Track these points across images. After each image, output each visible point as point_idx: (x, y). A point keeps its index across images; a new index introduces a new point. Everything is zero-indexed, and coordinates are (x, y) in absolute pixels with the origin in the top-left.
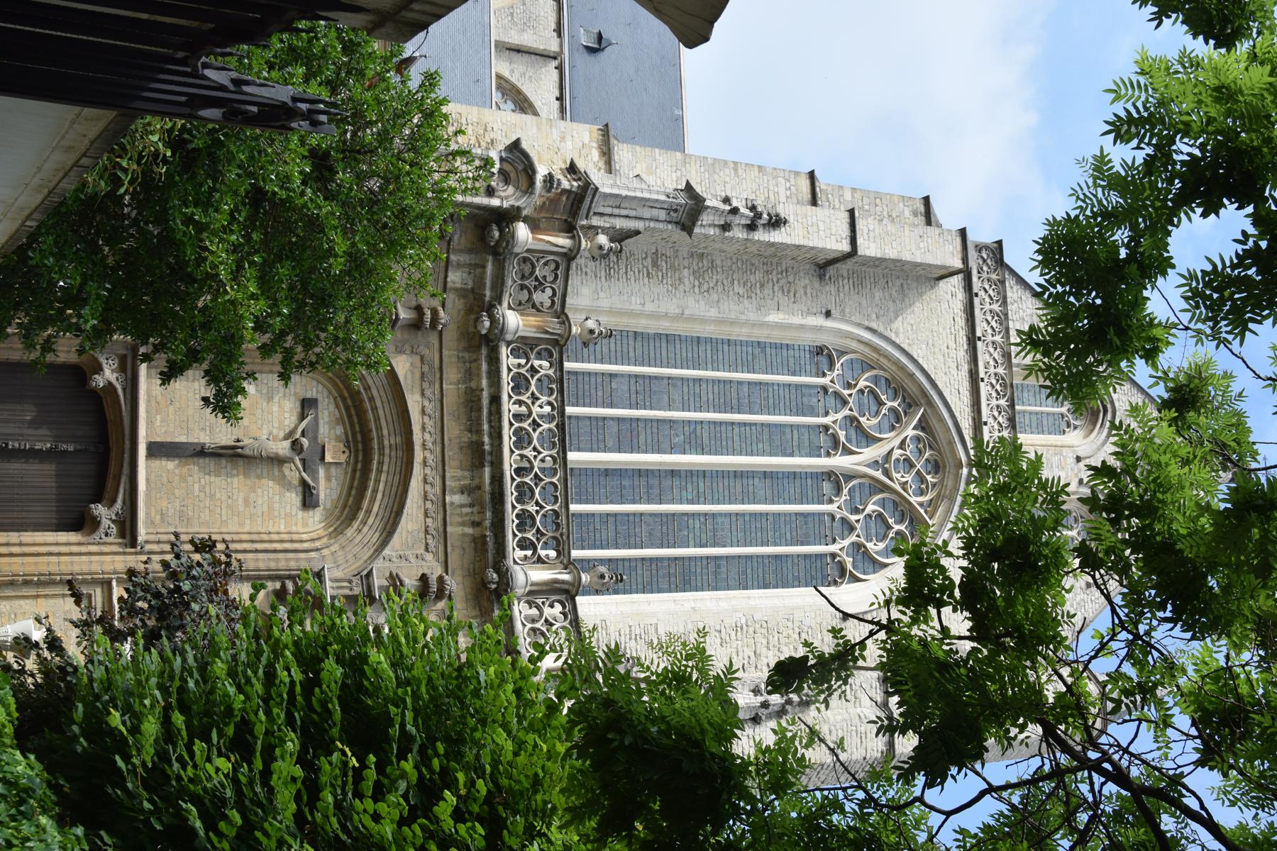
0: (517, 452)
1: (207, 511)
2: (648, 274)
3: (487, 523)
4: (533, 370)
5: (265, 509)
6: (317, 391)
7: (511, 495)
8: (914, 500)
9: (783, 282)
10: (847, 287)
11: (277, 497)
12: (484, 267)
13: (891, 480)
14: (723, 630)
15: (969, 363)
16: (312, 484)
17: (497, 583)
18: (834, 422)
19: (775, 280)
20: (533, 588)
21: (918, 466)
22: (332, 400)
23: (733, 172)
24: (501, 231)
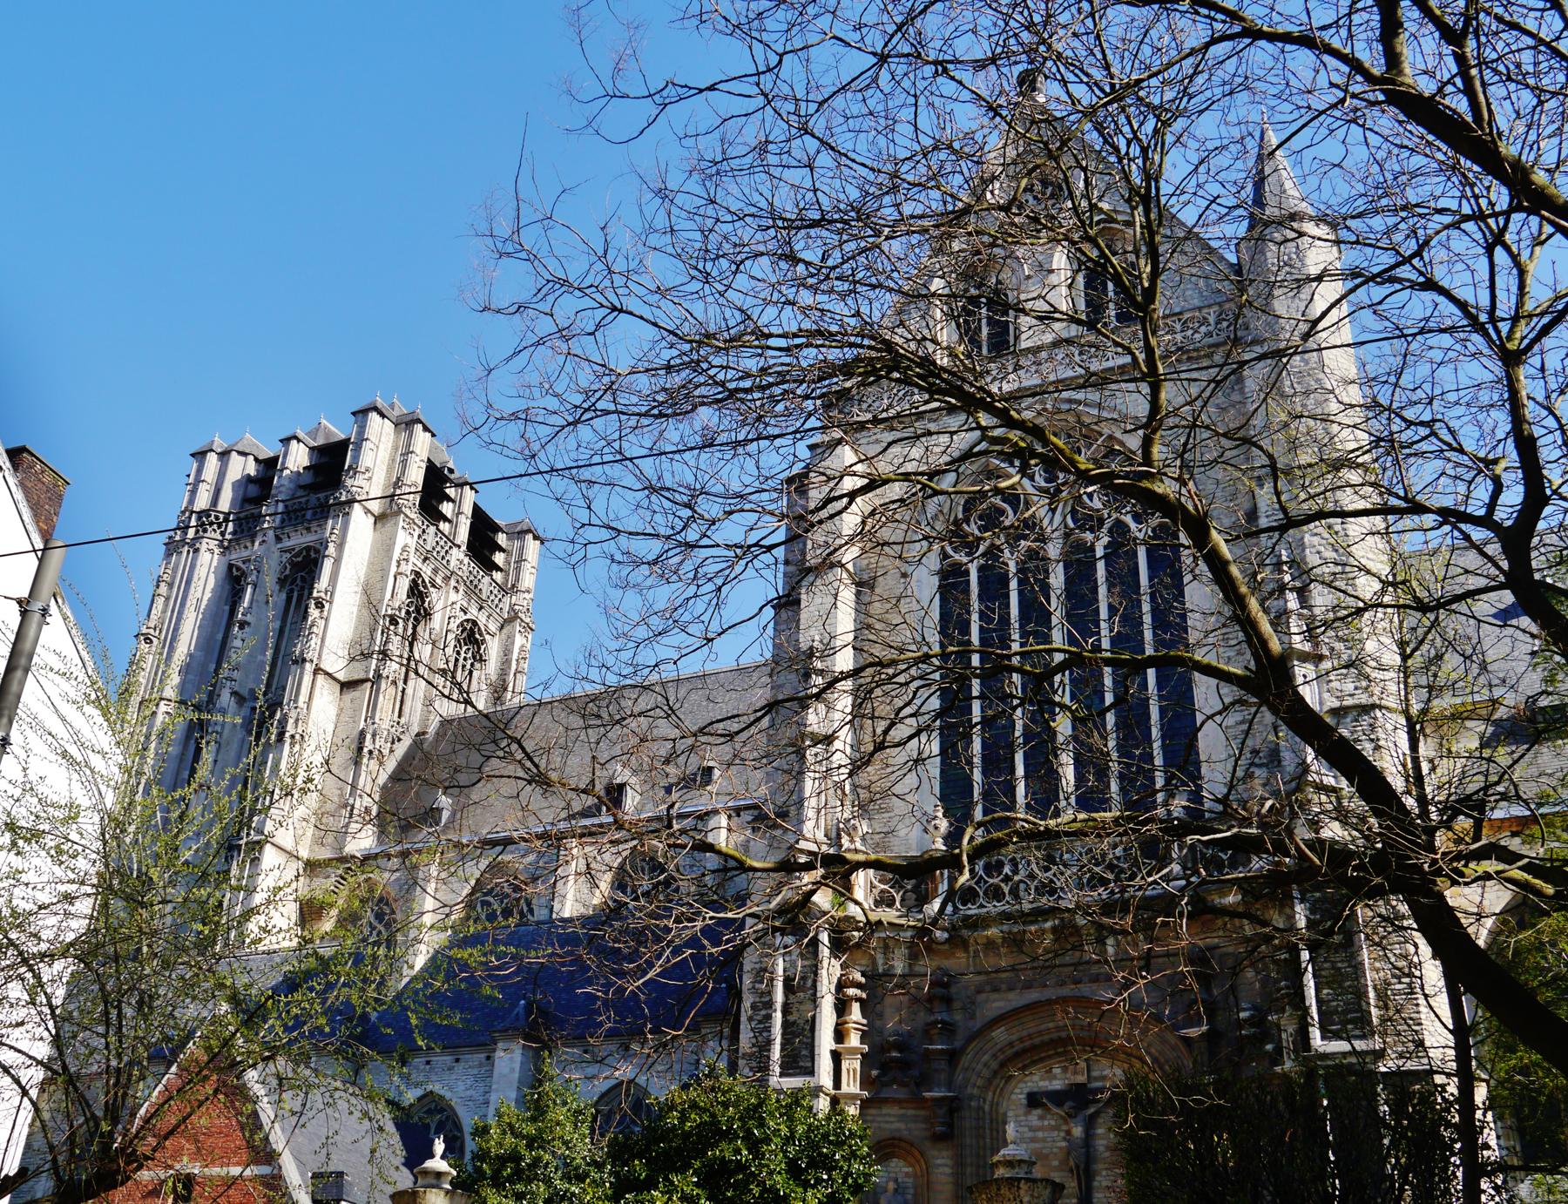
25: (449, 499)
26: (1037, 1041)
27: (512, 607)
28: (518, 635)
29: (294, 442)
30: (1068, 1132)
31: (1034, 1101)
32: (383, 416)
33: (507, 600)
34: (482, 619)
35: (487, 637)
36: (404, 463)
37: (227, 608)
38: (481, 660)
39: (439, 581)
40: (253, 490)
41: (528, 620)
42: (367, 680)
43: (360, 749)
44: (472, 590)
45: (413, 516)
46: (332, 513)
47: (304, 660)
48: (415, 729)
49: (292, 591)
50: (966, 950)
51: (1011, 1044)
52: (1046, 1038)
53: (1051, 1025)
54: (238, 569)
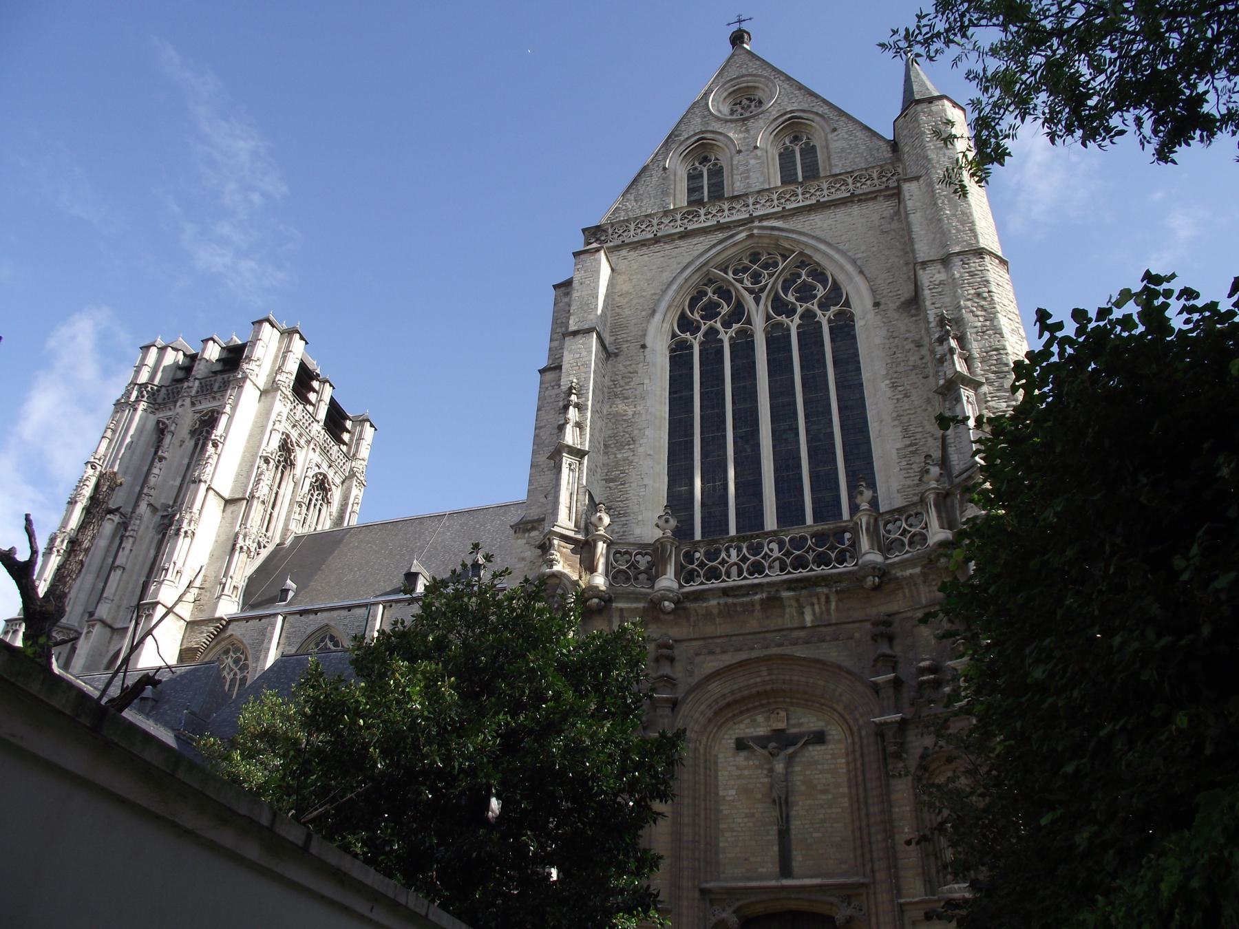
0: (767, 571)
1: (835, 825)
2: (622, 484)
3: (825, 590)
4: (702, 565)
5: (829, 776)
6: (730, 739)
7: (804, 573)
8: (781, 267)
9: (622, 383)
10: (623, 335)
11: (819, 767)
12: (621, 610)
13: (767, 285)
14: (897, 397)
15: (673, 240)
16: (806, 738)
17: (874, 577)
18: (726, 333)
19: (620, 389)
20: (876, 548)
21: (755, 267)
22: (737, 726)
23: (543, 429)
25: (314, 391)
26: (746, 693)
27: (352, 469)
28: (354, 487)
29: (211, 342)
30: (771, 770)
31: (741, 745)
32: (273, 326)
33: (348, 464)
34: (330, 474)
35: (333, 487)
36: (284, 358)
37: (153, 450)
38: (329, 503)
39: (302, 442)
40: (180, 374)
41: (362, 478)
42: (244, 499)
43: (234, 545)
44: (325, 452)
45: (287, 393)
46: (231, 386)
47: (200, 481)
48: (278, 541)
49: (199, 439)
50: (688, 619)
51: (724, 696)
52: (754, 691)
53: (758, 680)
54: (164, 423)
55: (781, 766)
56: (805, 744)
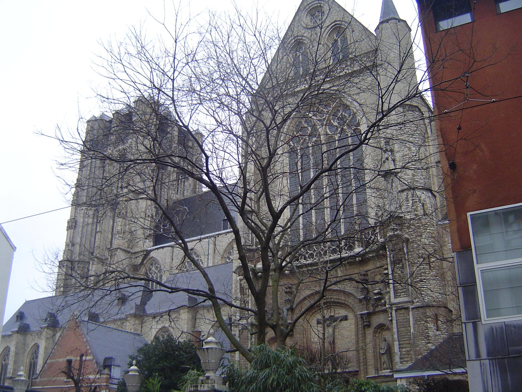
24: (258, 273)
55: (331, 330)
56: (340, 321)
